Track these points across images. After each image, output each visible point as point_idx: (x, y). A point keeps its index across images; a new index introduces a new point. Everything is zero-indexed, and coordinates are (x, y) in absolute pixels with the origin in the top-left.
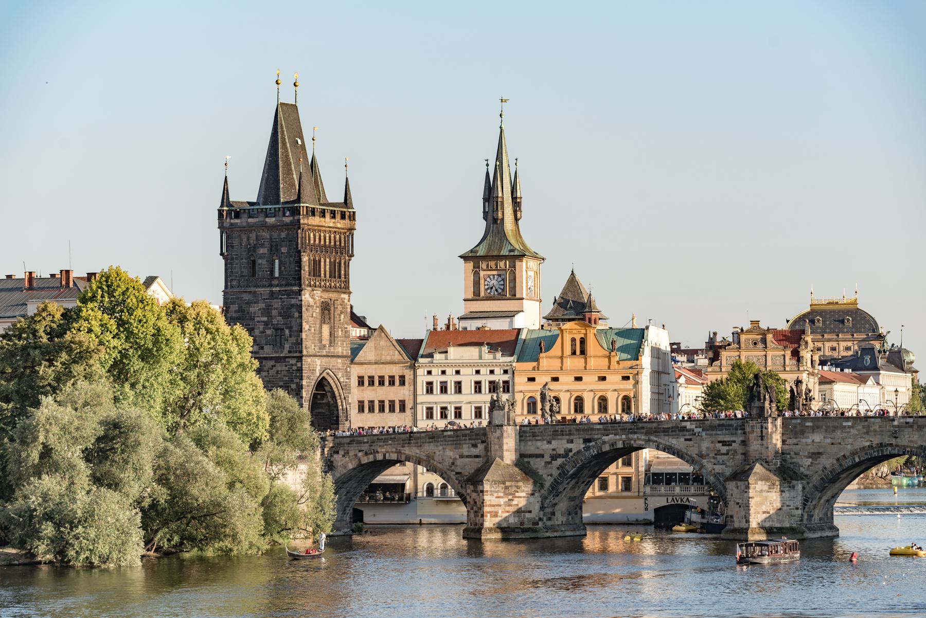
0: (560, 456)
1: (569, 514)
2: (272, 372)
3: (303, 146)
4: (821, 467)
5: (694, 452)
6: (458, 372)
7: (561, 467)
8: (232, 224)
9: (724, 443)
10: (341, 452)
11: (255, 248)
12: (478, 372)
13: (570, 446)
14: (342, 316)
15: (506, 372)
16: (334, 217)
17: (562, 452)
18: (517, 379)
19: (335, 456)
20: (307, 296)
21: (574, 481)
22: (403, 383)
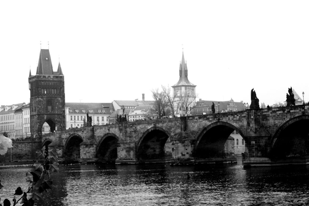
3: (49, 60)
8: (30, 81)
12: (139, 117)
14: (57, 103)
17: (66, 137)
20: (40, 98)
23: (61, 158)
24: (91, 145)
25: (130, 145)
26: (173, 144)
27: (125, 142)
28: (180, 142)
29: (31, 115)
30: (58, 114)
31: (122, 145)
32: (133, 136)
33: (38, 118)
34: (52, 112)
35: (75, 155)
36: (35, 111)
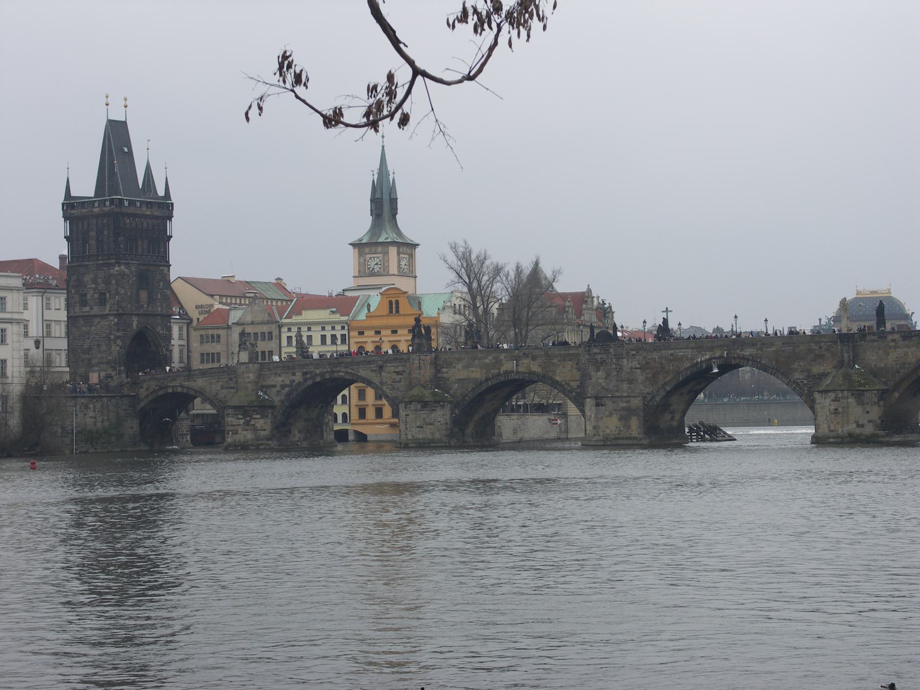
0: (286, 386)
3: (130, 153)
5: (376, 380)
6: (309, 329)
9: (398, 373)
10: (145, 387)
12: (323, 329)
13: (294, 378)
16: (152, 208)
17: (288, 382)
19: (141, 390)
20: (123, 267)
22: (271, 338)
23: (268, 439)
24: (439, 402)
25: (628, 402)
26: (836, 400)
28: (852, 395)
29: (72, 314)
30: (161, 315)
31: (609, 403)
33: (117, 324)
34: (150, 309)
35: (297, 432)
36: (102, 302)
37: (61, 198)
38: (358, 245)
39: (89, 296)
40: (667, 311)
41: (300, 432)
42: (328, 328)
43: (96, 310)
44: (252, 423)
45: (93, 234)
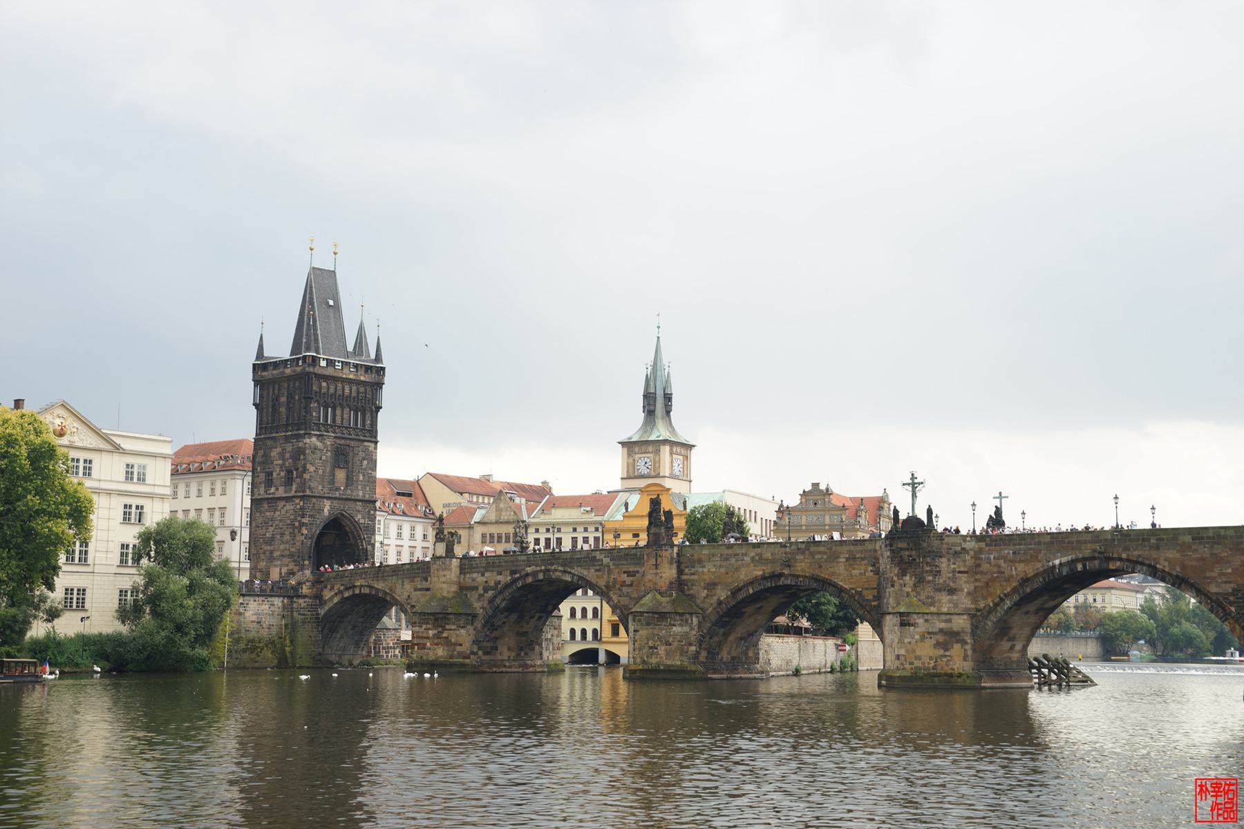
0: (491, 588)
1: (521, 649)
2: (283, 512)
3: (337, 308)
4: (715, 598)
5: (602, 583)
7: (491, 601)
11: (277, 398)
12: (575, 530)
13: (499, 578)
14: (365, 462)
15: (597, 530)
17: (492, 584)
18: (606, 537)
20: (314, 439)
21: (514, 617)
25: (949, 621)
27: (933, 609)
29: (256, 497)
31: (920, 621)
32: (962, 590)
33: (302, 508)
34: (349, 492)
36: (289, 481)
37: (252, 359)
38: (628, 445)
39: (275, 475)
40: (1000, 496)
41: (509, 649)
42: (580, 529)
43: (281, 492)
44: (445, 635)
45: (283, 399)
